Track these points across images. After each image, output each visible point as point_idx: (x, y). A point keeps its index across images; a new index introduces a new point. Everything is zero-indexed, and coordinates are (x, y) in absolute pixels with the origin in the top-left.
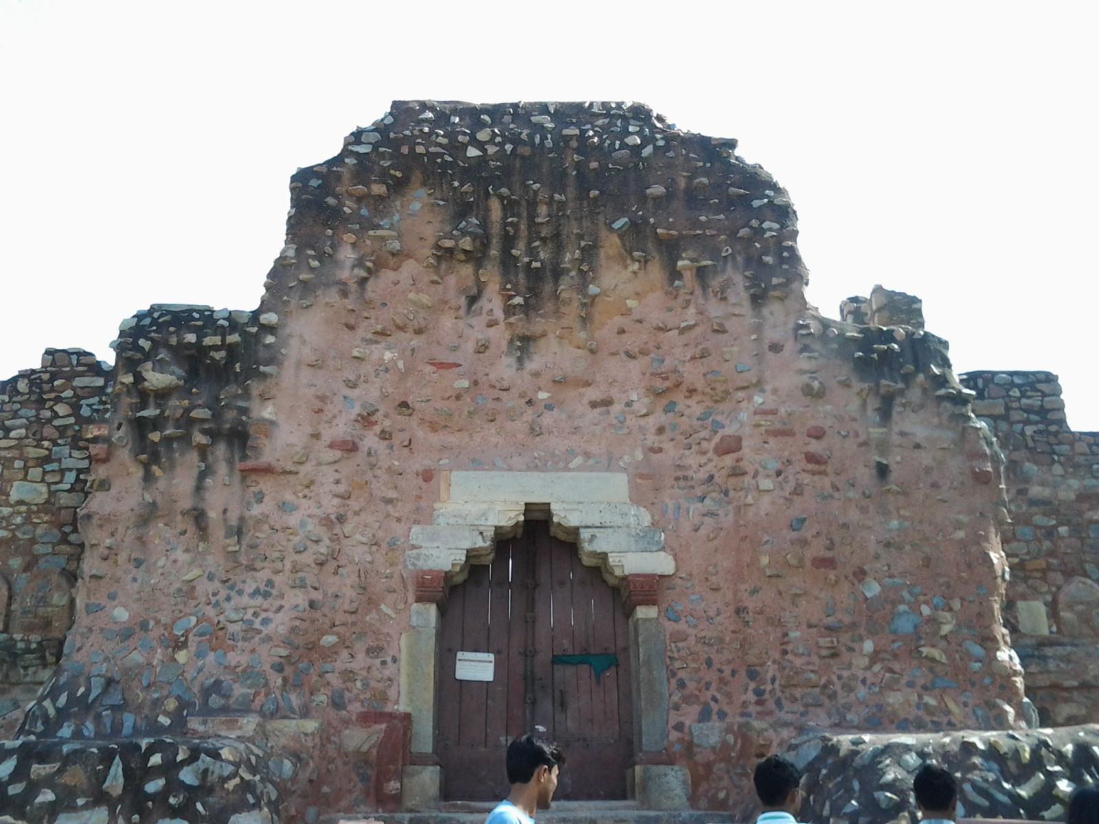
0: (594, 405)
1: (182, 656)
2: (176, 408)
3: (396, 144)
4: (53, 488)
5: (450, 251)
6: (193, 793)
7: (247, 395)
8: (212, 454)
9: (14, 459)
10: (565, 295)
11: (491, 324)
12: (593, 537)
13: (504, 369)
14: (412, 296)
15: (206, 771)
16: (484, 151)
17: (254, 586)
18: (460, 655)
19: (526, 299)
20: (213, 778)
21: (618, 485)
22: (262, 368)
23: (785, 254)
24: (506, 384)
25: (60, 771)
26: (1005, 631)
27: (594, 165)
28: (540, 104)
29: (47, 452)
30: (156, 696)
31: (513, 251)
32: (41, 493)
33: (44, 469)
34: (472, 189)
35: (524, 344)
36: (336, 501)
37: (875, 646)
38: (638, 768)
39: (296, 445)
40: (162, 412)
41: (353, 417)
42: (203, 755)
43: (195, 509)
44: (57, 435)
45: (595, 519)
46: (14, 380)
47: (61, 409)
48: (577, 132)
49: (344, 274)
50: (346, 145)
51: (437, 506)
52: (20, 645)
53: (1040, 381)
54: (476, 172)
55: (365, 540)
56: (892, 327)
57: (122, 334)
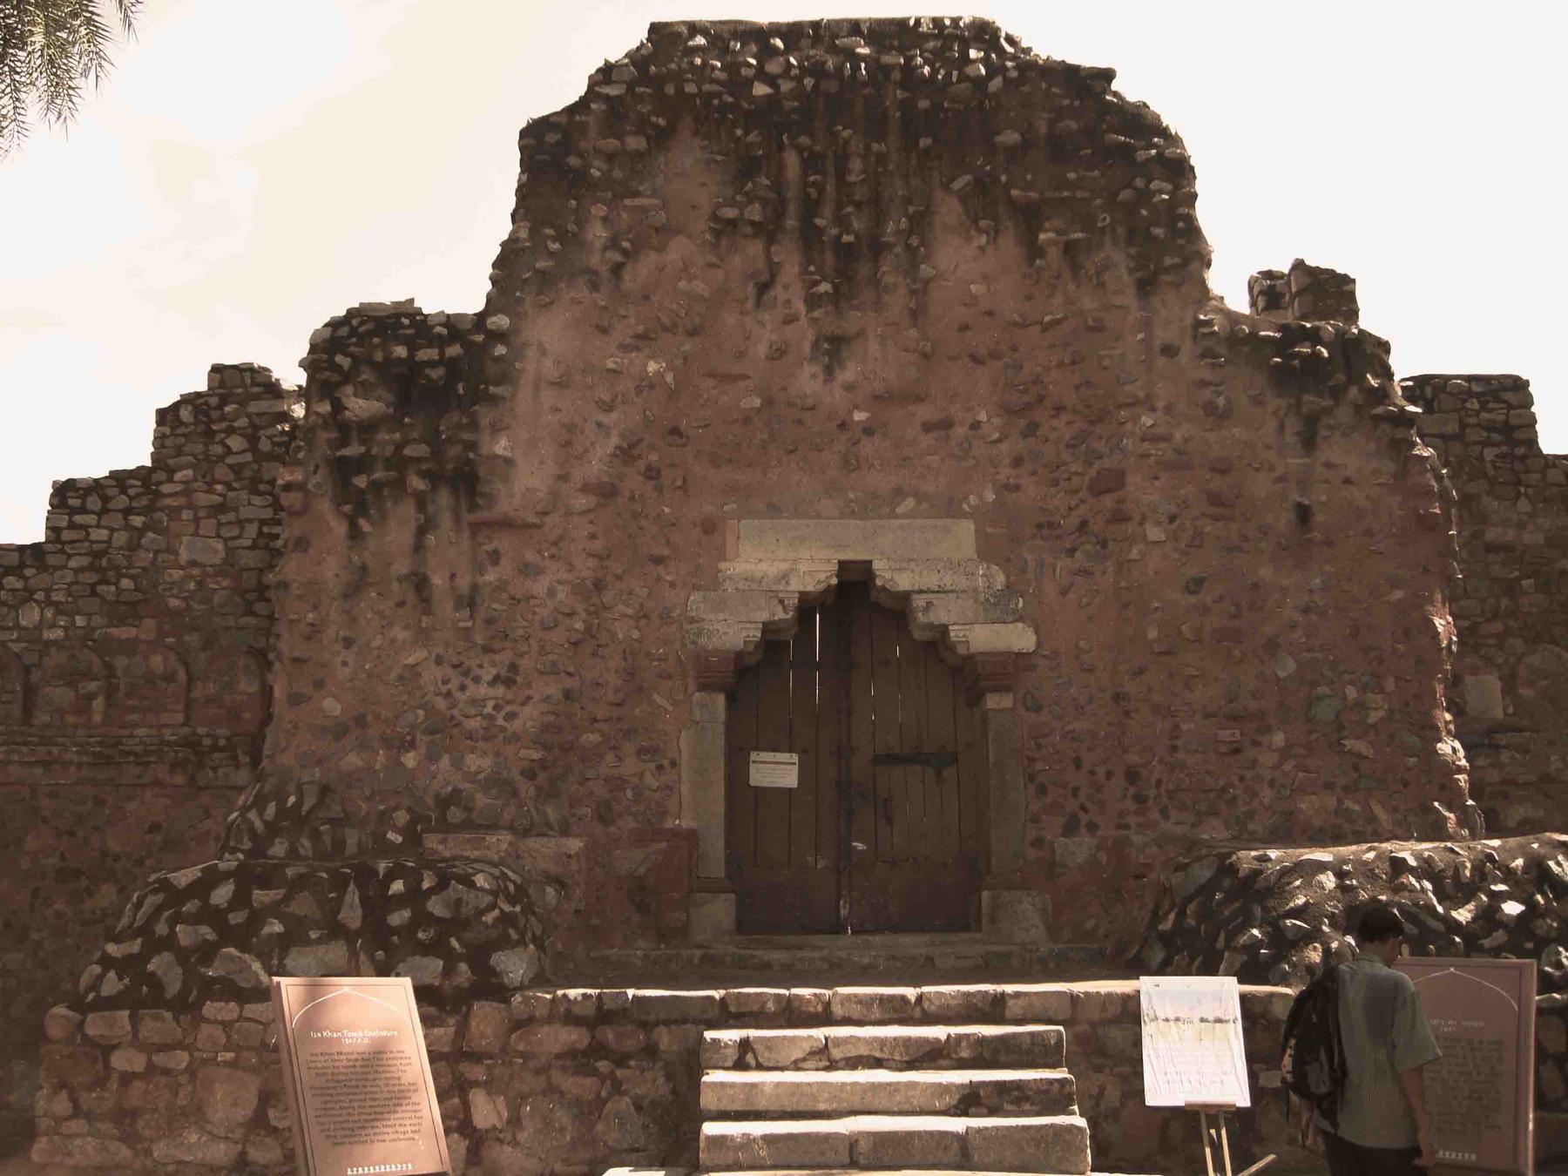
0: (928, 427)
1: (410, 760)
2: (386, 442)
3: (657, 82)
4: (231, 544)
5: (732, 223)
6: (448, 926)
7: (474, 425)
8: (433, 502)
10: (888, 280)
11: (790, 320)
12: (929, 604)
13: (807, 381)
14: (682, 284)
15: (459, 902)
17: (494, 671)
18: (754, 756)
19: (836, 287)
20: (466, 910)
22: (492, 389)
23: (1181, 224)
24: (809, 402)
25: (287, 899)
26: (1448, 717)
27: (924, 104)
28: (849, 21)
29: (221, 499)
30: (382, 807)
31: (818, 221)
32: (216, 552)
33: (218, 521)
34: (760, 139)
35: (833, 348)
36: (592, 562)
37: (1287, 740)
38: (985, 894)
39: (538, 490)
40: (368, 451)
41: (610, 451)
42: (453, 882)
43: (414, 574)
44: (231, 477)
45: (932, 581)
46: (176, 406)
47: (235, 443)
49: (594, 261)
50: (593, 82)
51: (722, 565)
52: (207, 742)
53: (1505, 389)
54: (768, 115)
55: (630, 611)
56: (1317, 323)
57: (314, 348)
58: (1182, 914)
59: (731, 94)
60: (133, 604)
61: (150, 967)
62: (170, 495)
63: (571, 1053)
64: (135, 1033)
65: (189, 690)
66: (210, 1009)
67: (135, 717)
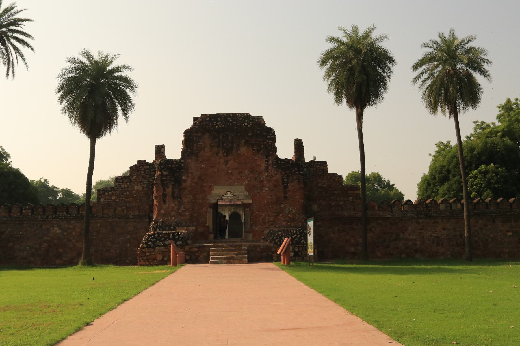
1: (173, 218)
4: (143, 187)
5: (213, 146)
6: (182, 238)
9: (134, 182)
16: (219, 127)
19: (227, 154)
25: (164, 235)
32: (141, 188)
35: (226, 162)
45: (239, 194)
48: (235, 123)
51: (212, 192)
52: (142, 215)
53: (323, 164)
58: (265, 236)
61: (149, 243)
62: (133, 180)
66: (156, 248)
67: (131, 212)
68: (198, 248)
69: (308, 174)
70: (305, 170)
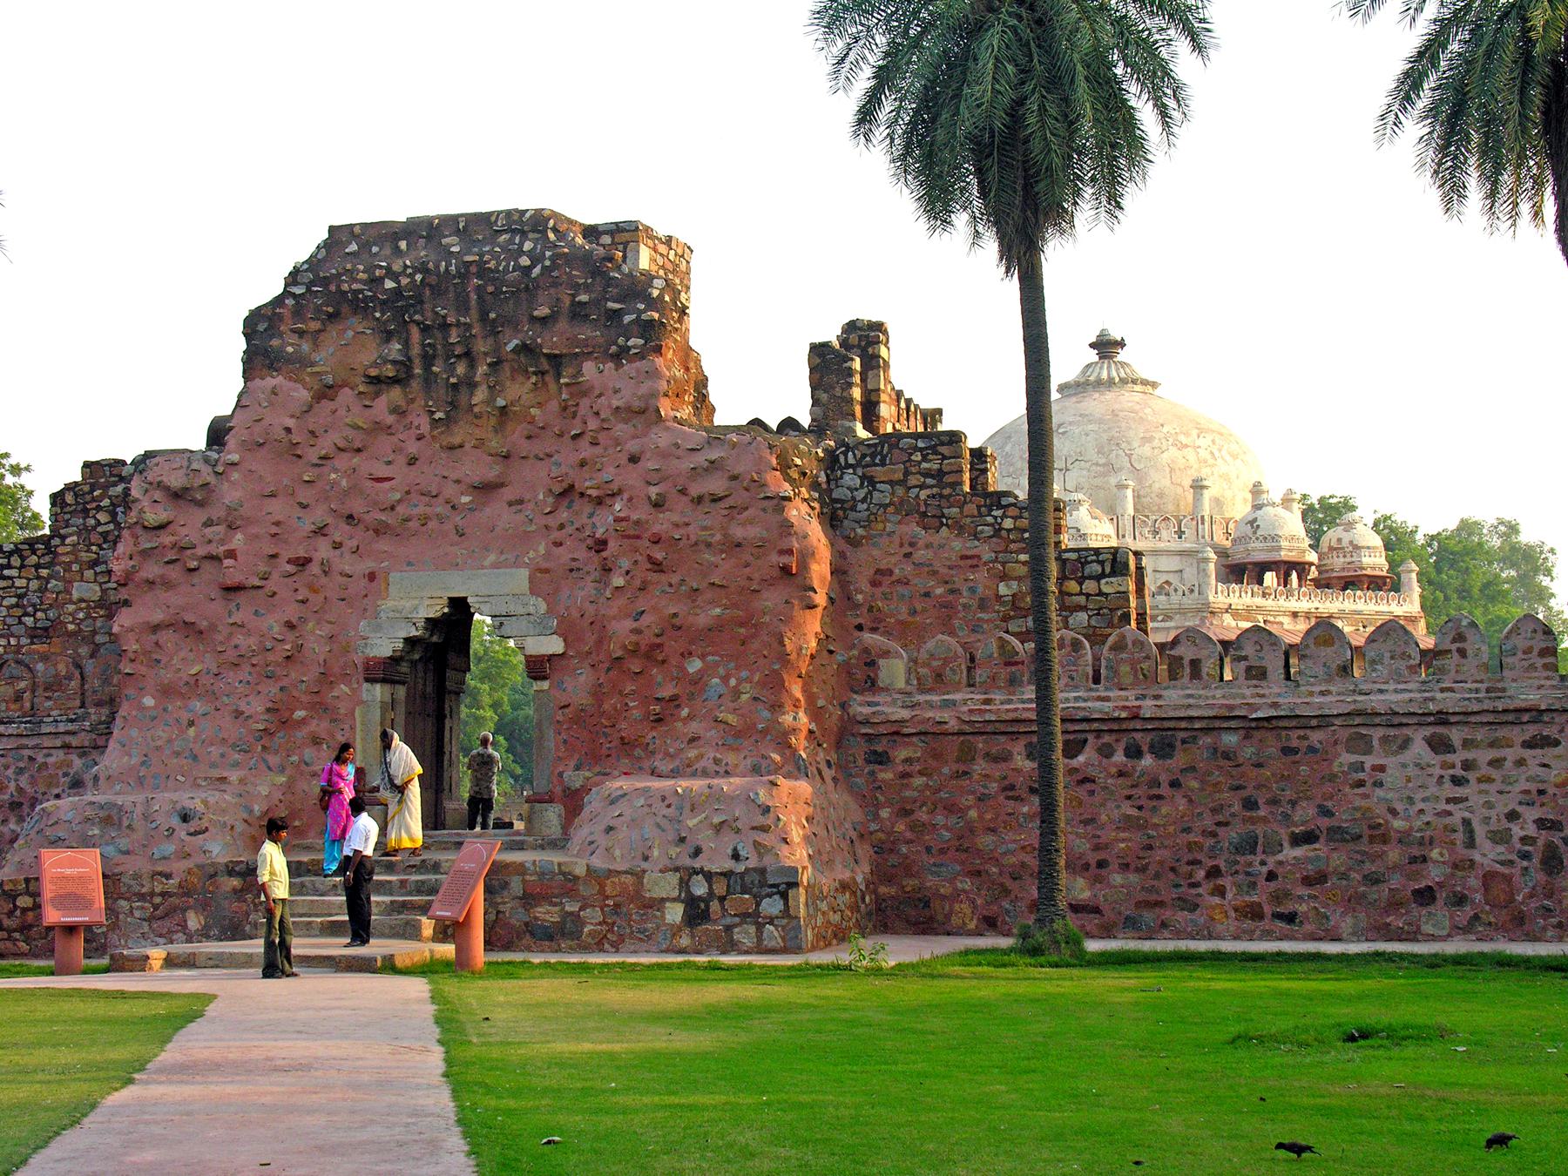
3: (325, 282)
4: (104, 586)
12: (502, 624)
16: (398, 282)
19: (447, 413)
21: (520, 578)
27: (490, 289)
31: (434, 368)
47: (103, 517)
50: (286, 285)
53: (942, 444)
59: (370, 290)
60: (46, 629)
63: (235, 891)
64: (27, 887)
65: (83, 685)
67: (50, 703)
68: (239, 874)
69: (863, 500)
70: (847, 477)
